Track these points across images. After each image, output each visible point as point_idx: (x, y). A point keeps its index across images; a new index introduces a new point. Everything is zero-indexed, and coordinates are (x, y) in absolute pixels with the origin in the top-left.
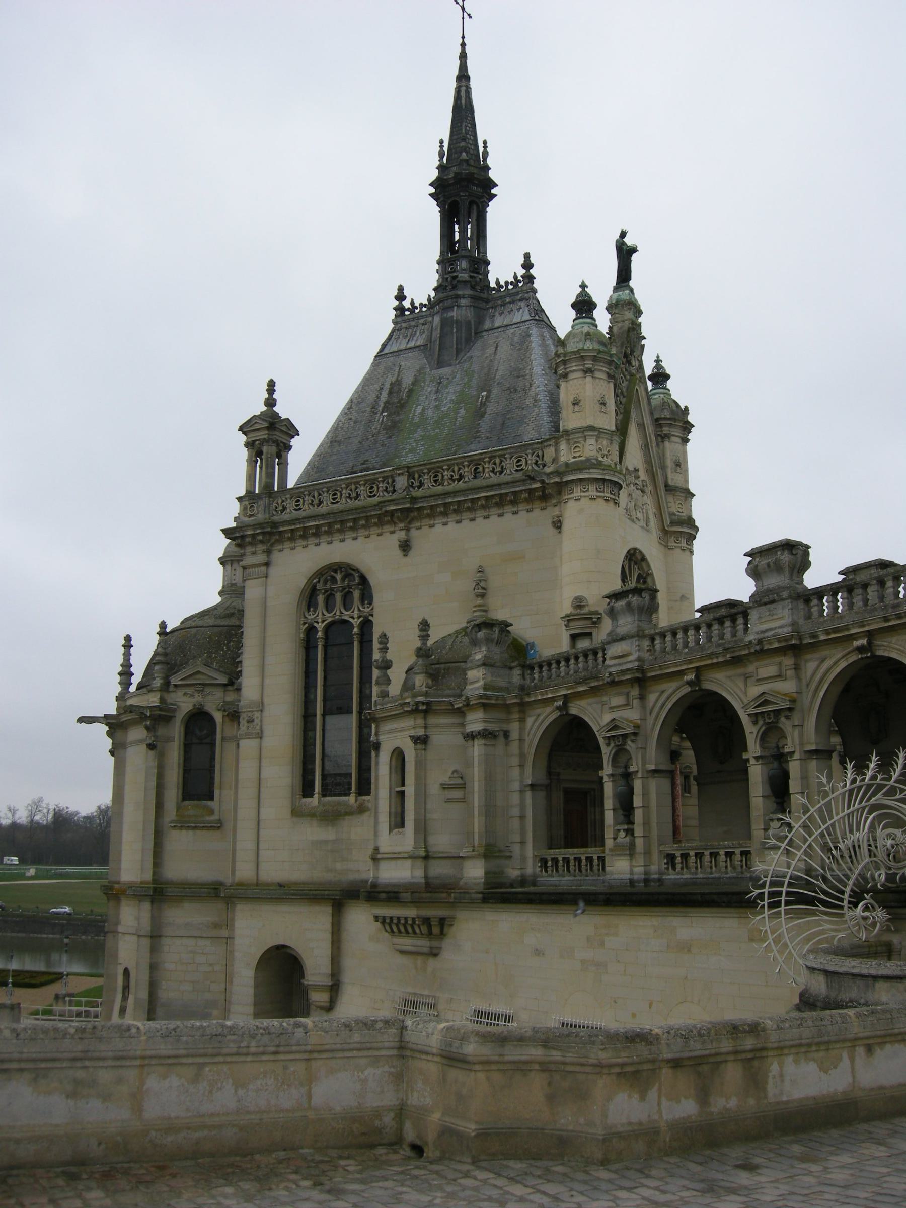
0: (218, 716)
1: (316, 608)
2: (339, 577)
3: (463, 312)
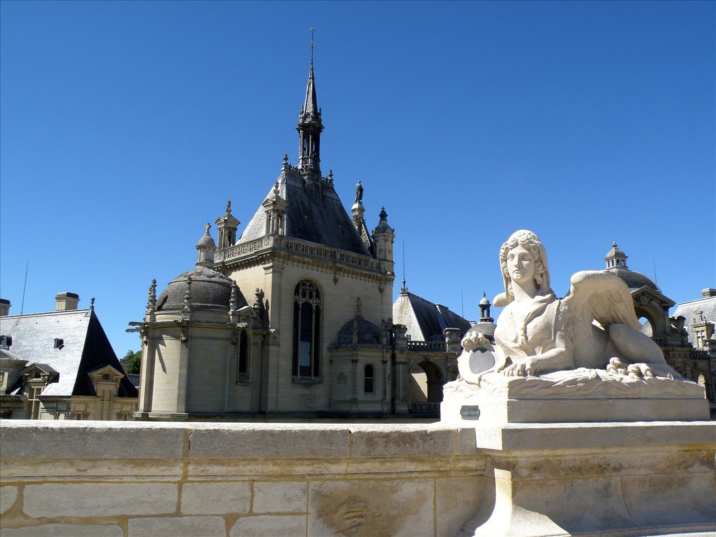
1: (298, 295)
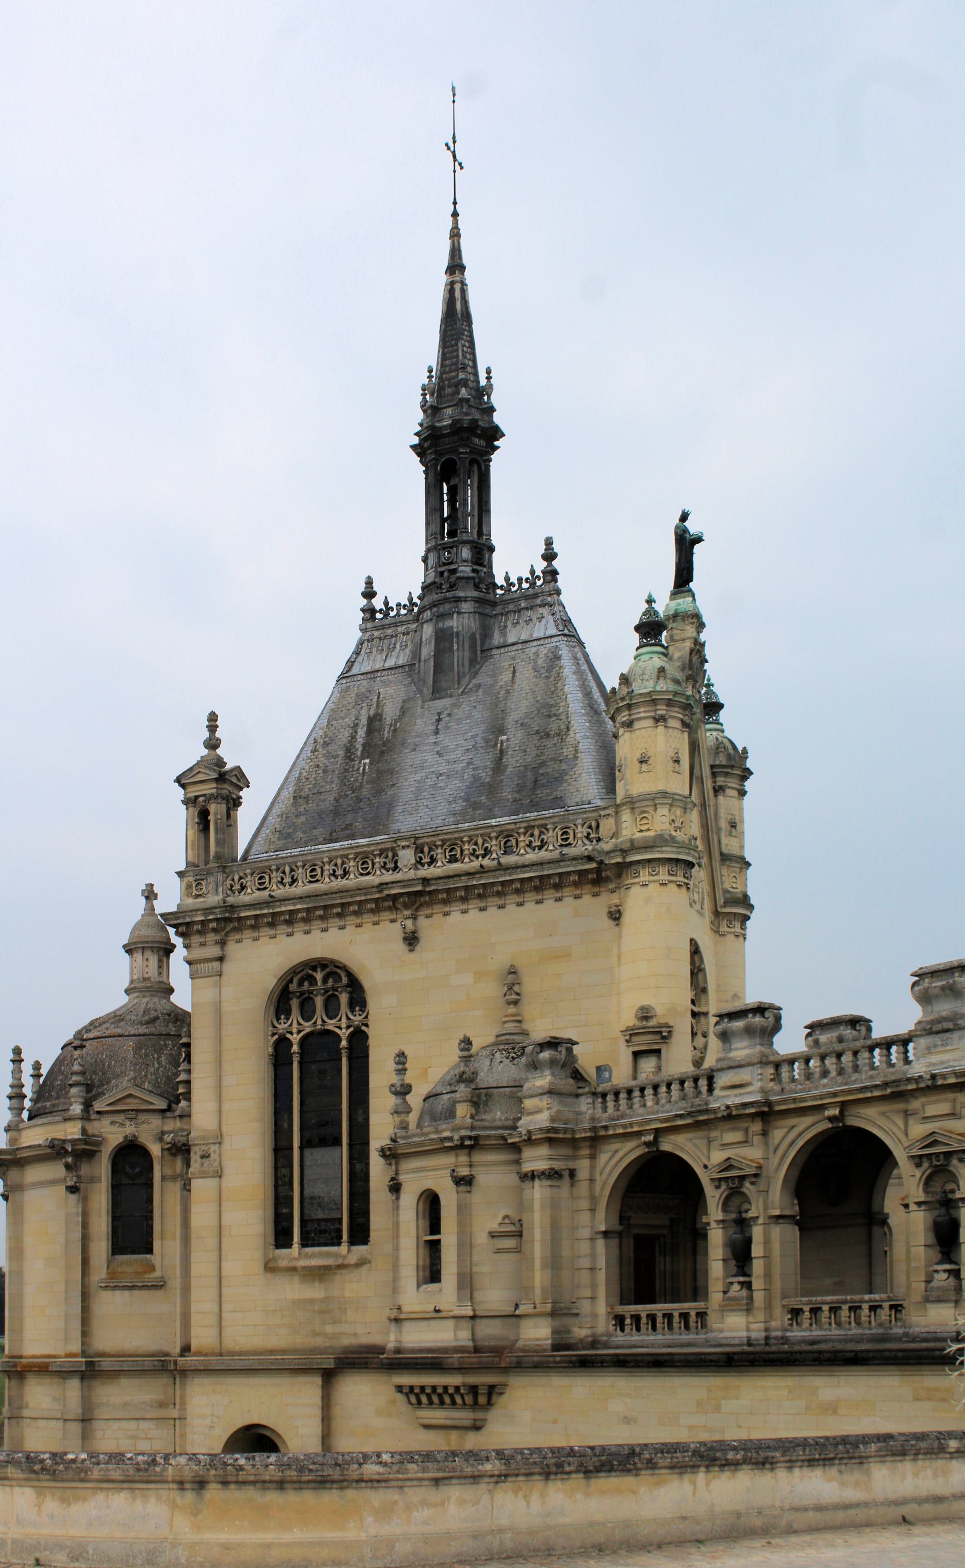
0: (155, 1150)
1: (288, 1014)
2: (319, 976)
3: (466, 621)
